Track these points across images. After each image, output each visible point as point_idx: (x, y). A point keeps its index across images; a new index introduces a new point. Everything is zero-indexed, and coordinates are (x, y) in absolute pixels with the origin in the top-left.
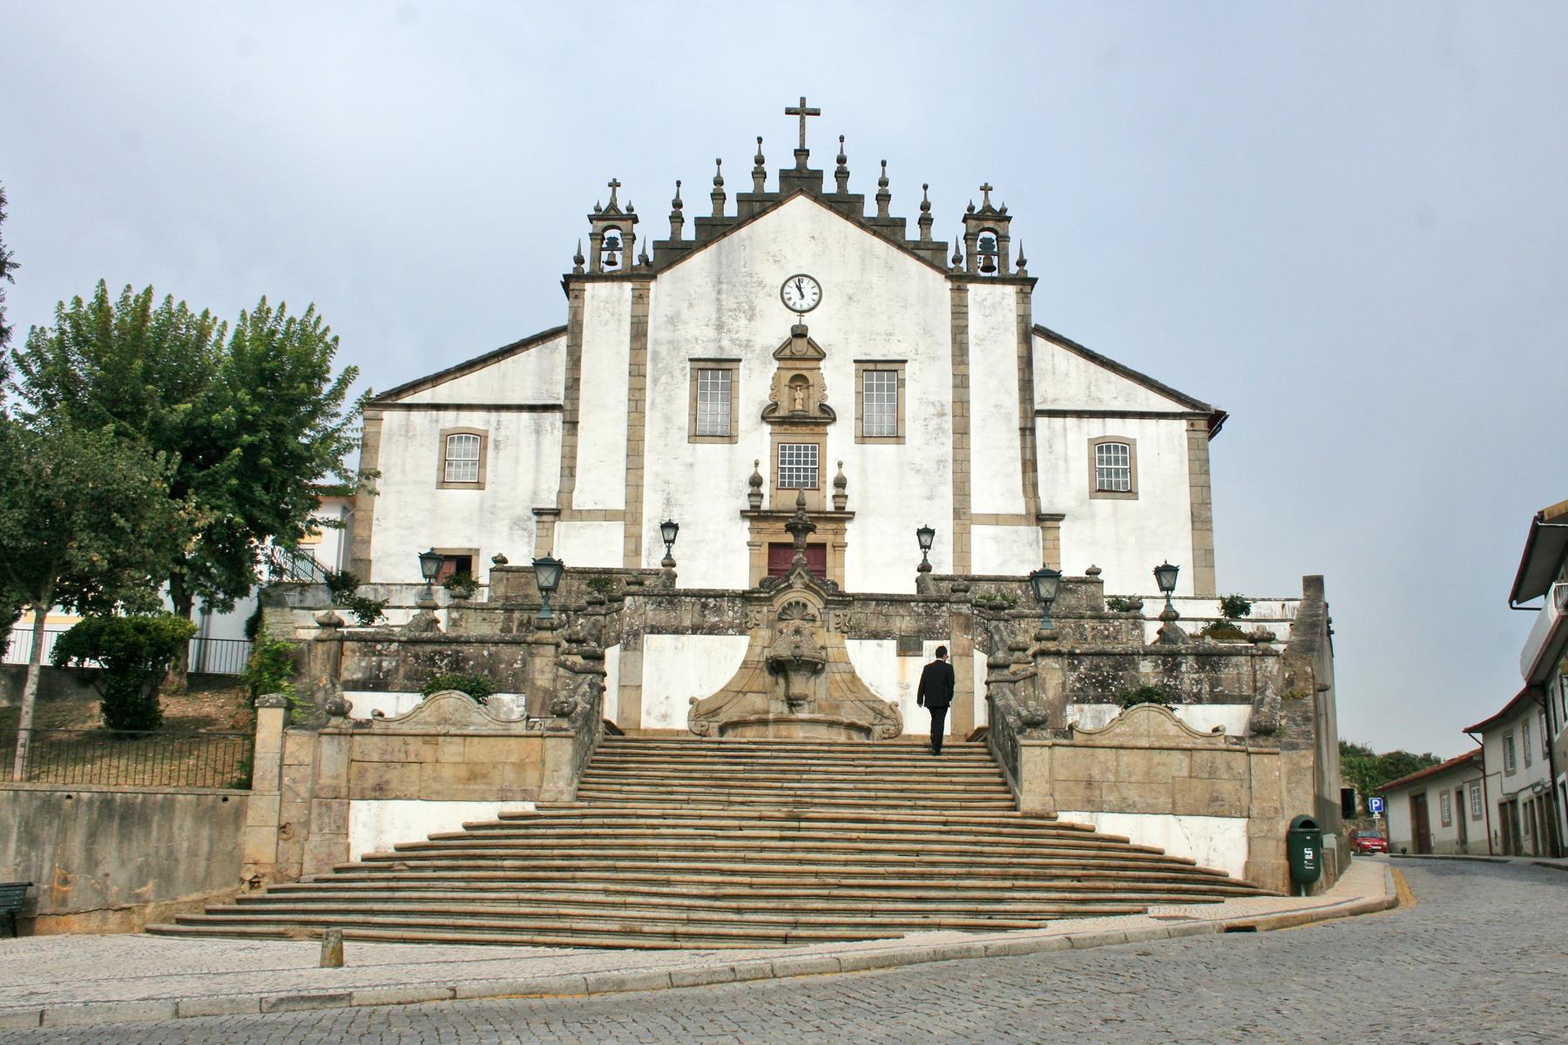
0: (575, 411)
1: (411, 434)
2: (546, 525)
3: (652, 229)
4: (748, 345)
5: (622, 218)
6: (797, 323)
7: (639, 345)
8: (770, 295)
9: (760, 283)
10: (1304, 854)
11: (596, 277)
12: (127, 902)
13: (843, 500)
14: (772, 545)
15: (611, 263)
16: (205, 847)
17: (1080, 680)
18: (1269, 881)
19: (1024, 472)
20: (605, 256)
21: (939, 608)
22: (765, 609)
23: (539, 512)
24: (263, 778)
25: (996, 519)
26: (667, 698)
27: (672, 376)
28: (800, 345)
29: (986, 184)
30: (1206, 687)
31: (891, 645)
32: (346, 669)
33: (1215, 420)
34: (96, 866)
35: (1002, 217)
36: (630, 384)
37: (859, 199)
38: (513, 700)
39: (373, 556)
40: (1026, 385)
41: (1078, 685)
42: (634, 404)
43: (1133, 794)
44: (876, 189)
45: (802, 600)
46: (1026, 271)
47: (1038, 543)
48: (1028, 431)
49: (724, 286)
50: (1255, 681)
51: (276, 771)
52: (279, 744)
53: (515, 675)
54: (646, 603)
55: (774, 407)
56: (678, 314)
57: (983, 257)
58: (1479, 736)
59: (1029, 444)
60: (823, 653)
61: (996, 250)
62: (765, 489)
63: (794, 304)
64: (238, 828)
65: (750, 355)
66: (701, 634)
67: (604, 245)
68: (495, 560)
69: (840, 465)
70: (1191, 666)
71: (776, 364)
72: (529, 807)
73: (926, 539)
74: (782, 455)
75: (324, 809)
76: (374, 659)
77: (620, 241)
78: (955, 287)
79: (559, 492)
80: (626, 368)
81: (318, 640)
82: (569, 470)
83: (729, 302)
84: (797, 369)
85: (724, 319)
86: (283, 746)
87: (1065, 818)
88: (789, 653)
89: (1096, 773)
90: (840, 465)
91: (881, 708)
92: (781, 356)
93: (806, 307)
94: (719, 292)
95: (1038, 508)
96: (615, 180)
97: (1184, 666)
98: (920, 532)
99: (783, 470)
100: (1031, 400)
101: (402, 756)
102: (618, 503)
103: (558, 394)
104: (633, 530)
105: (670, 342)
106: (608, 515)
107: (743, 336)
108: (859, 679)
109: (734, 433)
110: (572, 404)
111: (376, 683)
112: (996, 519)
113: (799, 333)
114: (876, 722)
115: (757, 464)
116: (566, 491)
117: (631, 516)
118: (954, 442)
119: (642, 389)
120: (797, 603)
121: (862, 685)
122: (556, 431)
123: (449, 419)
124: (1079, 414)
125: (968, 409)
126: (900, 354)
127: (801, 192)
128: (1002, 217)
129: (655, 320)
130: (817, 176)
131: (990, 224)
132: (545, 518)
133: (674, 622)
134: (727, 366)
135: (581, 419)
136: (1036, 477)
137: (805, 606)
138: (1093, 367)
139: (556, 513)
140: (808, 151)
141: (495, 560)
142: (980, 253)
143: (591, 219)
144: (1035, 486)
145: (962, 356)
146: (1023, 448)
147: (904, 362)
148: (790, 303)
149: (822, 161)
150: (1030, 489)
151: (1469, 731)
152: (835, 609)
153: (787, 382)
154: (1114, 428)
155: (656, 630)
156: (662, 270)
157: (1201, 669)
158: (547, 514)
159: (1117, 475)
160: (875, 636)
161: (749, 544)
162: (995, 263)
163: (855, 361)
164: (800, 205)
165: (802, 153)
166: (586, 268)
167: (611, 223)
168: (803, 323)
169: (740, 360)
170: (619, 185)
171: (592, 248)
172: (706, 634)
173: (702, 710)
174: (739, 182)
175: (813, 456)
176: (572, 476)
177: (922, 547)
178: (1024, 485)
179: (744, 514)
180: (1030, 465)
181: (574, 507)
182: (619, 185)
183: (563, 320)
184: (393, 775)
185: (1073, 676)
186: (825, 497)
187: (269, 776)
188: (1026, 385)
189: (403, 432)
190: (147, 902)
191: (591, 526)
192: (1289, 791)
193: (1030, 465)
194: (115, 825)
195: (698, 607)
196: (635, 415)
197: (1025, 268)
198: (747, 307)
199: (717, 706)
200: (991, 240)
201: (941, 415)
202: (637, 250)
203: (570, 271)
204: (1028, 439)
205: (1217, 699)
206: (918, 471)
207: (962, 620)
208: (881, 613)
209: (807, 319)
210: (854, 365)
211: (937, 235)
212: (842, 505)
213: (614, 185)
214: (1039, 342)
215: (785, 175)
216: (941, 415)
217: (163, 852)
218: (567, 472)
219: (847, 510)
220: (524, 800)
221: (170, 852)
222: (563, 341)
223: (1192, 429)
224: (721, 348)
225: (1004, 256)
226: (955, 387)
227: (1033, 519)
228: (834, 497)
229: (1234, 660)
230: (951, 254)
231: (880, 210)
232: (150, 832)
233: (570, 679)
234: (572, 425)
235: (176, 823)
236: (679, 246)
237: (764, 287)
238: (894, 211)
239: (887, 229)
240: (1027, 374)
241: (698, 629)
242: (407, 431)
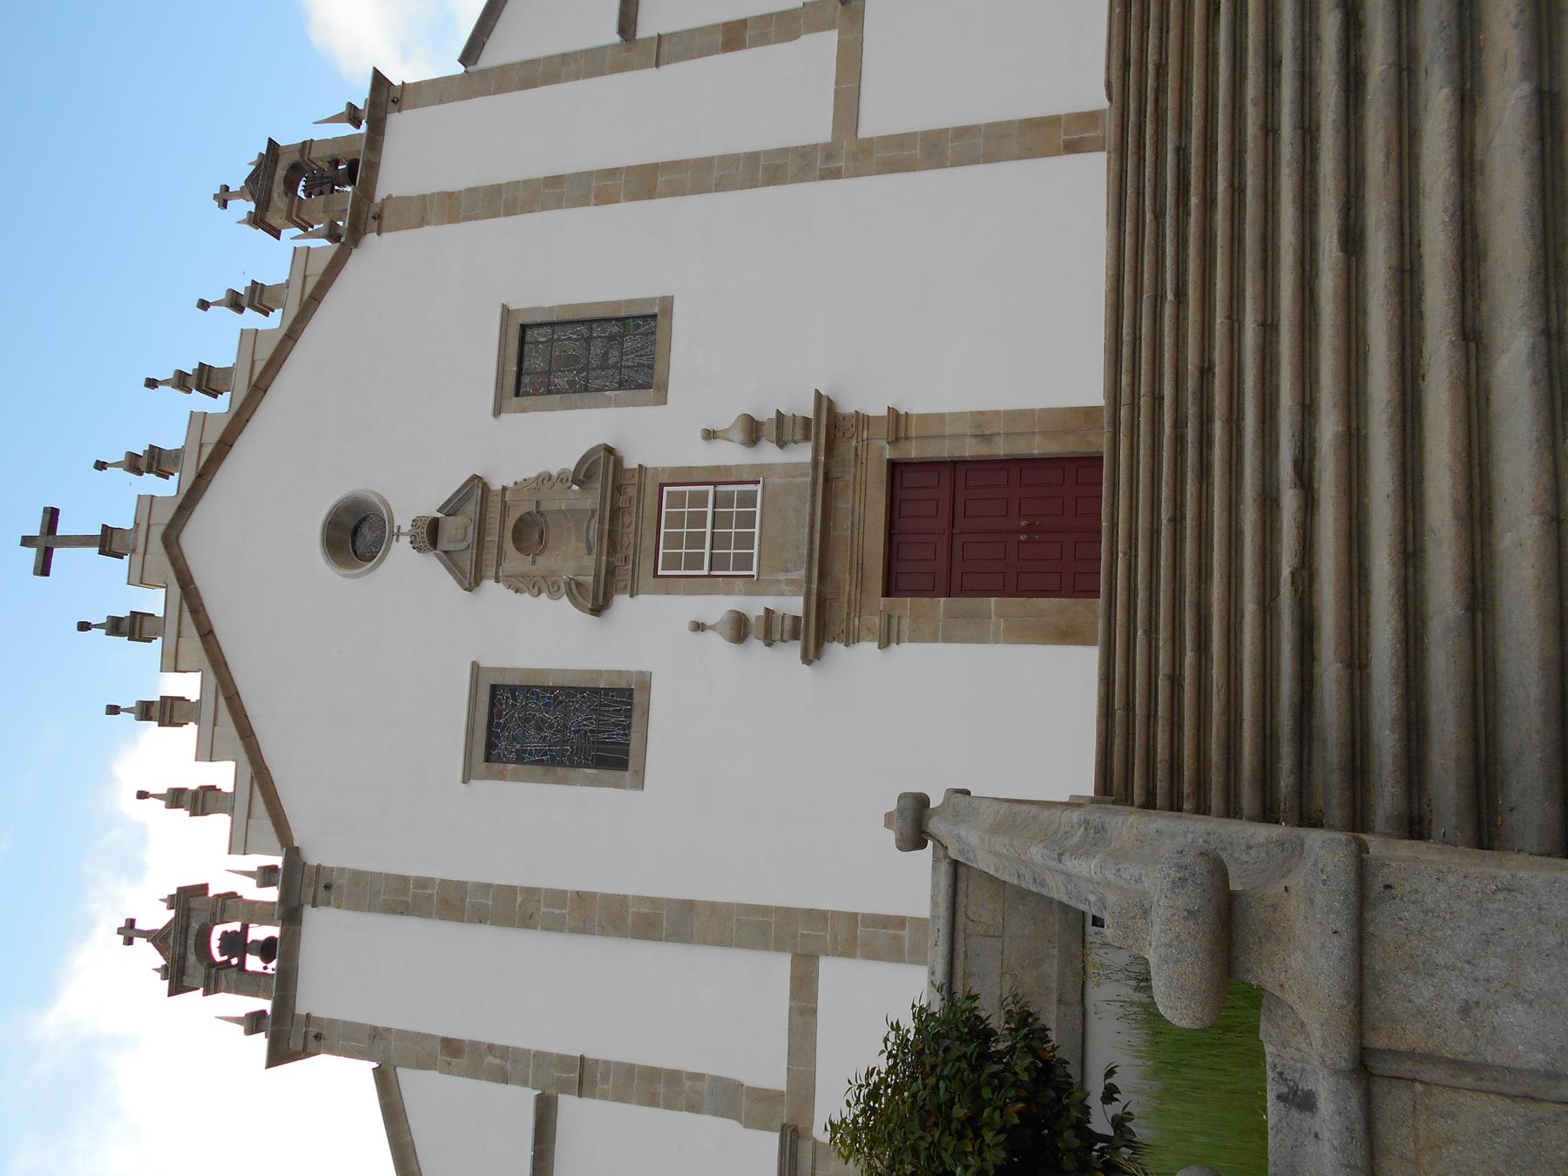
11: (284, 987)
14: (887, 592)
15: (267, 949)
20: (254, 963)
28: (453, 532)
48: (663, 51)
55: (575, 591)
57: (336, 188)
62: (755, 607)
69: (710, 435)
78: (375, 224)
90: (710, 435)
113: (430, 534)
115: (699, 627)
161: (885, 643)
164: (193, 540)
165: (108, 542)
167: (191, 942)
179: (812, 655)
183: (358, 1075)
202: (251, 891)
210: (504, 416)
212: (799, 423)
214: (492, 57)
219: (811, 415)
228: (781, 444)
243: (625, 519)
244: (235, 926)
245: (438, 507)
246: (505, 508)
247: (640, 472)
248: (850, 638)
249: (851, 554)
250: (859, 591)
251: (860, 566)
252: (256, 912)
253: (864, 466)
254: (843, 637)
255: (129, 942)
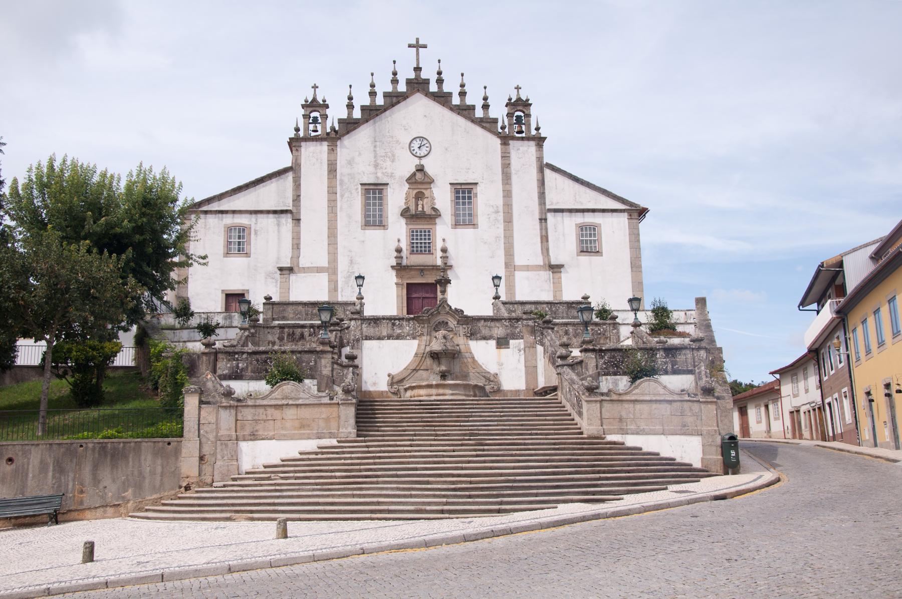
0: (299, 213)
1: (208, 227)
2: (285, 276)
3: (337, 113)
4: (392, 176)
5: (320, 106)
6: (418, 163)
7: (332, 176)
8: (403, 148)
9: (397, 141)
10: (730, 454)
11: (307, 139)
12: (117, 501)
13: (446, 259)
16: (159, 469)
17: (605, 363)
18: (713, 467)
19: (542, 242)
20: (311, 127)
21: (517, 322)
22: (426, 325)
23: (281, 269)
24: (189, 431)
25: (527, 268)
26: (376, 374)
27: (351, 193)
28: (419, 176)
29: (518, 86)
30: (670, 366)
31: (493, 343)
32: (219, 368)
33: (642, 212)
34: (99, 483)
35: (526, 104)
36: (328, 198)
37: (450, 95)
38: (311, 383)
39: (189, 295)
40: (542, 195)
41: (604, 366)
42: (331, 208)
43: (643, 426)
44: (459, 89)
45: (446, 321)
46: (540, 133)
47: (550, 281)
48: (543, 220)
49: (378, 144)
50: (694, 362)
51: (196, 427)
52: (197, 413)
53: (311, 369)
54: (362, 324)
56: (353, 159)
58: (778, 376)
59: (544, 228)
60: (458, 348)
61: (523, 122)
62: (405, 253)
63: (416, 153)
64: (177, 458)
65: (393, 181)
66: (393, 339)
67: (311, 121)
68: (266, 298)
70: (662, 355)
72: (334, 442)
73: (496, 281)
74: (413, 234)
75: (224, 447)
76: (234, 362)
77: (319, 119)
79: (292, 257)
80: (326, 189)
81: (204, 353)
82: (296, 246)
83: (381, 152)
85: (378, 161)
86: (199, 414)
87: (610, 438)
88: (440, 348)
89: (624, 414)
90: (444, 240)
91: (488, 376)
92: (410, 181)
93: (422, 155)
94: (375, 147)
95: (549, 262)
96: (315, 84)
97: (658, 355)
98: (493, 278)
99: (413, 243)
100: (545, 204)
101: (264, 417)
102: (324, 262)
103: (289, 204)
104: (333, 277)
105: (349, 174)
106: (319, 270)
107: (389, 171)
108: (477, 361)
109: (386, 224)
110: (297, 209)
111: (237, 375)
112: (527, 268)
113: (421, 169)
114: (487, 383)
115: (399, 241)
116: (296, 256)
117: (332, 270)
118: (504, 227)
119: (335, 200)
120: (443, 322)
121: (479, 364)
122: (288, 224)
123: (229, 220)
124: (570, 211)
125: (511, 209)
126: (474, 180)
127: (418, 91)
128: (526, 104)
129: (340, 163)
130: (427, 82)
131: (520, 108)
132: (284, 272)
133: (378, 334)
134: (381, 187)
135: (303, 217)
136: (548, 245)
137: (447, 323)
138: (577, 186)
139: (291, 270)
140: (421, 68)
141: (266, 298)
142: (515, 124)
143: (303, 106)
144: (548, 250)
145: (507, 180)
146: (541, 229)
147: (476, 184)
148: (414, 152)
149: (428, 74)
150: (545, 250)
151: (772, 373)
152: (463, 325)
153: (414, 196)
154: (589, 219)
155: (368, 338)
156: (344, 135)
157: (667, 356)
158: (285, 270)
159: (587, 243)
160: (485, 338)
161: (396, 284)
162: (524, 129)
163: (450, 184)
165: (418, 69)
166: (301, 134)
168: (422, 163)
169: (388, 184)
170: (317, 87)
171: (304, 123)
172: (395, 339)
173: (395, 380)
174: (384, 86)
175: (429, 235)
176: (298, 248)
177: (495, 286)
178: (542, 249)
180: (545, 238)
181: (300, 266)
182: (317, 87)
183: (289, 164)
184: (260, 427)
185: (601, 362)
186: (436, 258)
187: (193, 430)
188: (542, 195)
189: (203, 226)
190: (129, 501)
191: (310, 275)
192: (722, 421)
193: (545, 238)
194: (109, 458)
195: (390, 325)
196: (333, 215)
197: (540, 131)
198: (390, 155)
199: (403, 377)
200: (521, 116)
201: (497, 212)
203: (293, 136)
204: (544, 224)
205: (675, 372)
206: (485, 243)
207: (529, 329)
208: (486, 326)
209: (424, 162)
210: (449, 185)
211: (492, 114)
213: (315, 87)
214: (547, 172)
215: (409, 82)
216: (497, 212)
217: (136, 473)
218: (295, 246)
220: (330, 438)
221: (140, 473)
222: (290, 176)
223: (630, 218)
224: (377, 178)
225: (528, 126)
226: (504, 197)
227: (547, 268)
229: (684, 352)
230: (500, 124)
231: (461, 100)
232: (128, 463)
233: (340, 370)
234: (297, 220)
235: (143, 458)
236: (352, 121)
238: (469, 101)
239: (465, 111)
240: (542, 189)
241: (391, 337)
242: (205, 226)
244: (320, 121)
246: (427, 189)
248: (397, 276)
252: (324, 128)
255: (313, 87)
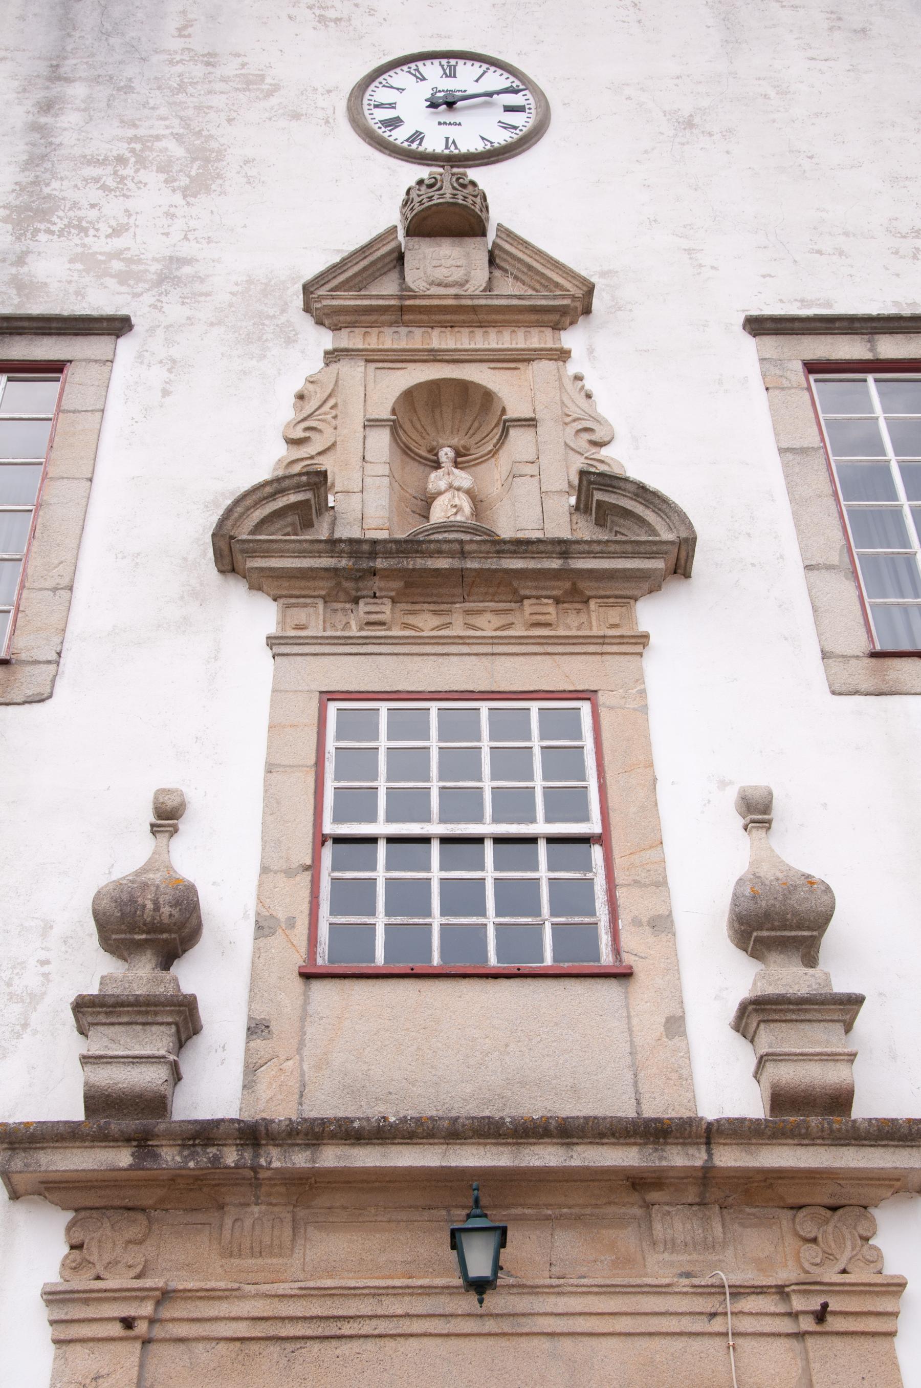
65: (175, 311)
71: (326, 340)
84: (434, 356)
94: (48, 106)
148: (399, 136)
210: (750, 343)
237: (269, 94)
243: (488, 616)
245: (506, 224)
247: (622, 640)
249: (378, 1293)
250: (242, 1329)
251: (332, 1329)
253: (699, 1325)
254: (84, 1282)
